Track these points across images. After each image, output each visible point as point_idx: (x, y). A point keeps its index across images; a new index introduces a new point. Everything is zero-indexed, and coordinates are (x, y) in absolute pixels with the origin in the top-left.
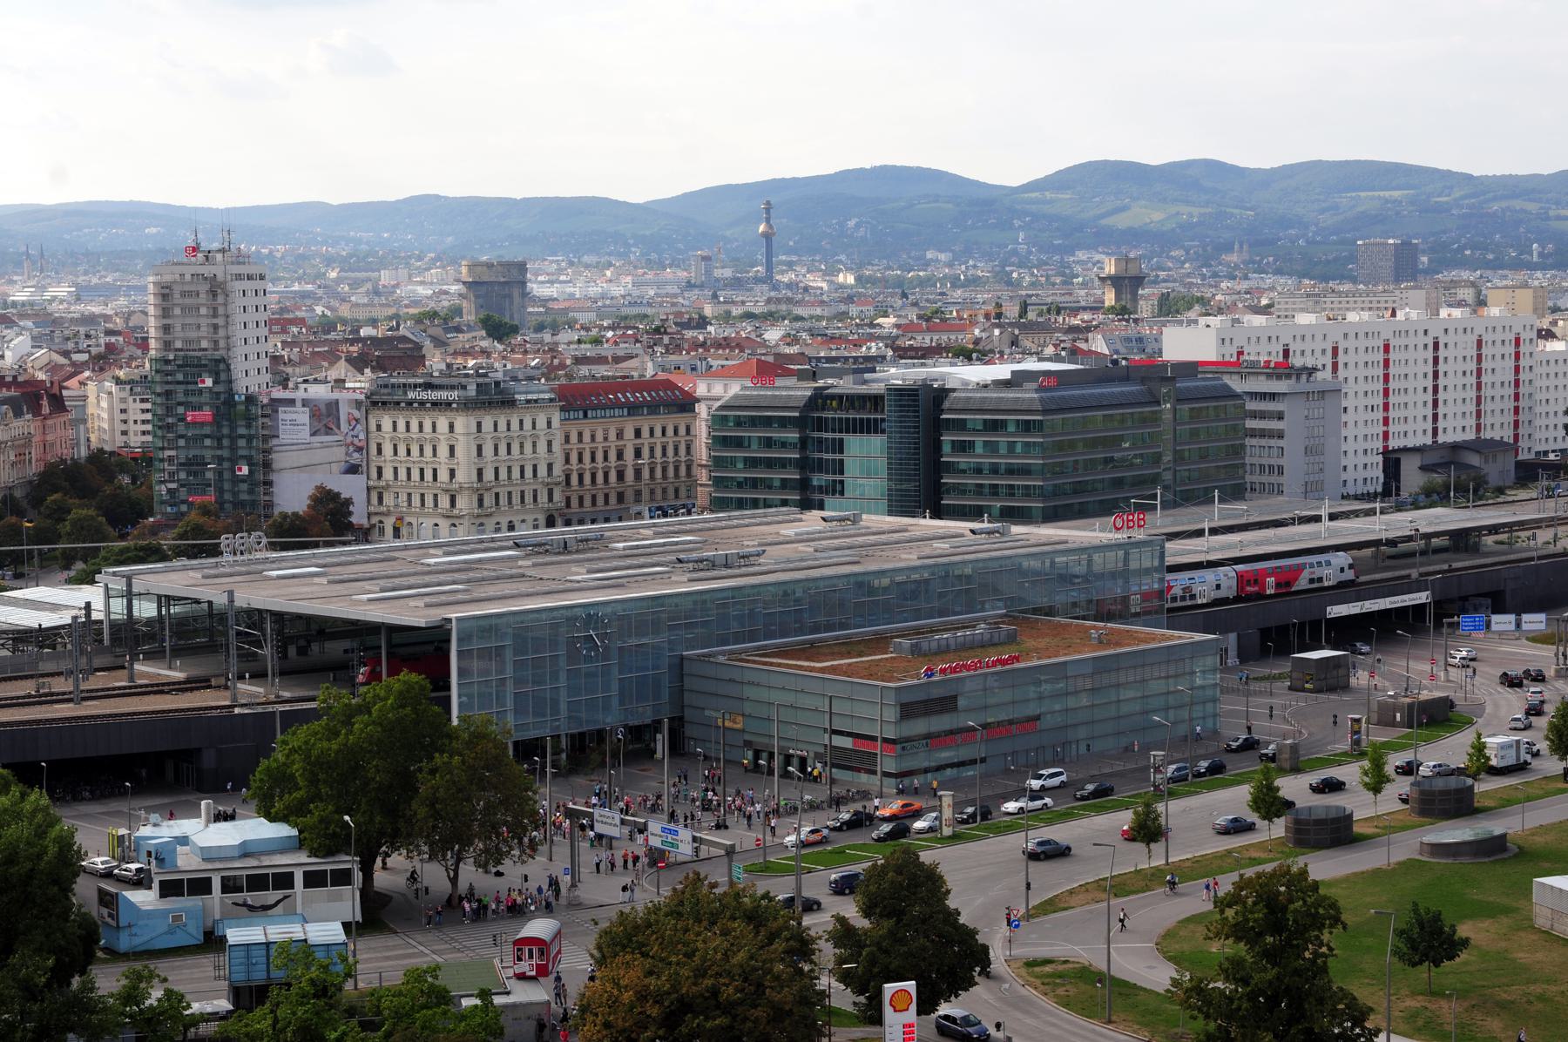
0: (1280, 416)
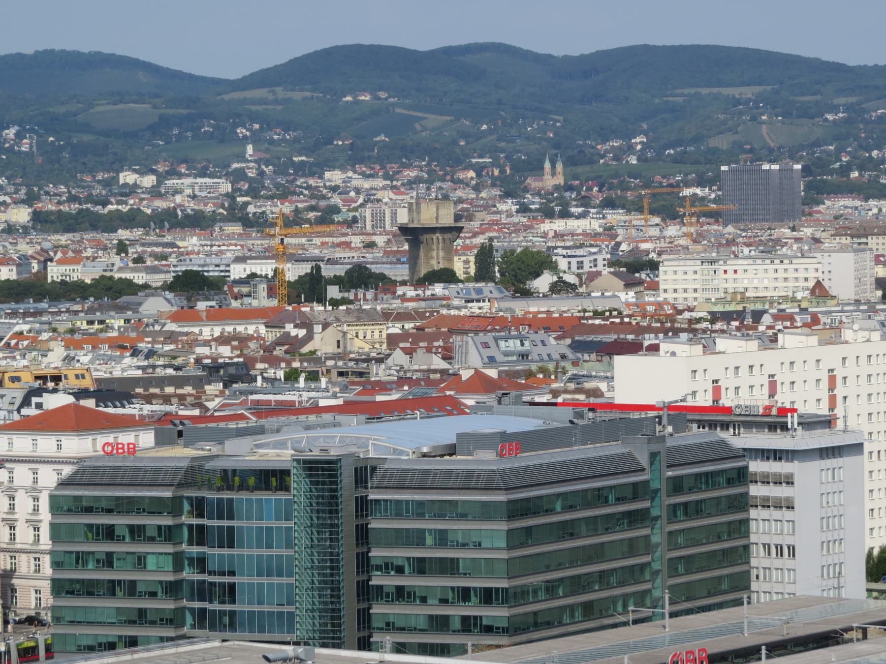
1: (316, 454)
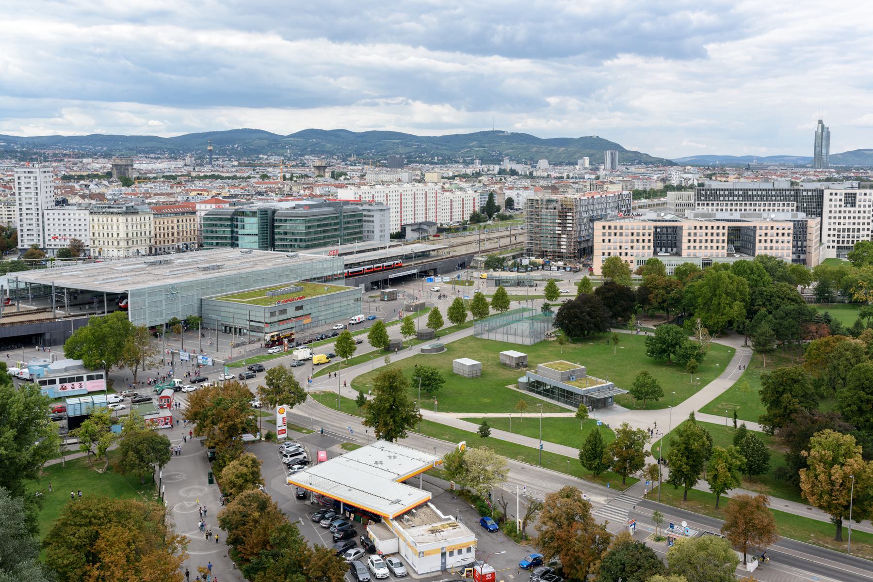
0: (373, 216)
1: (263, 208)
